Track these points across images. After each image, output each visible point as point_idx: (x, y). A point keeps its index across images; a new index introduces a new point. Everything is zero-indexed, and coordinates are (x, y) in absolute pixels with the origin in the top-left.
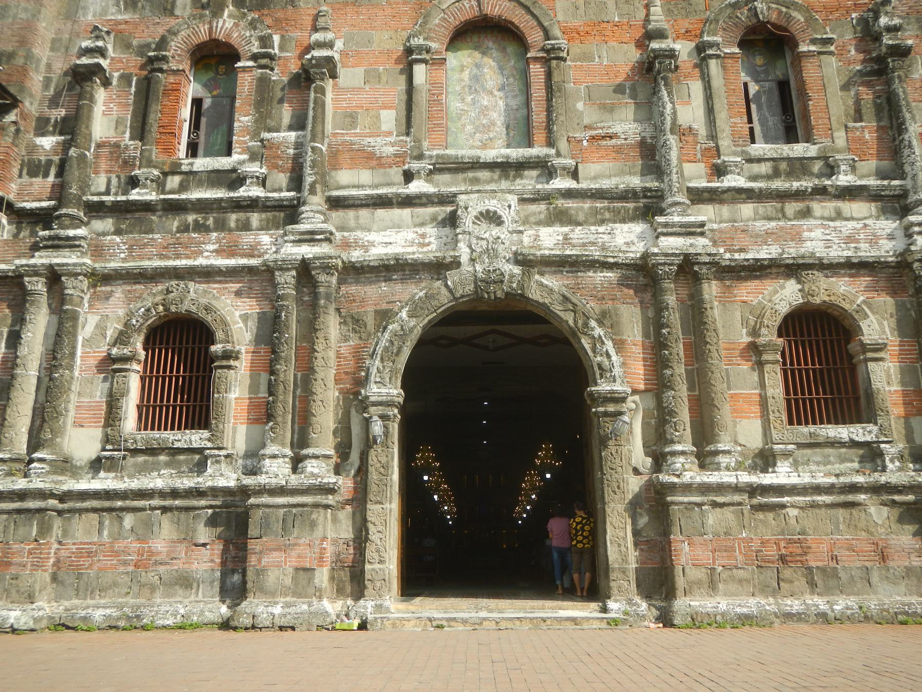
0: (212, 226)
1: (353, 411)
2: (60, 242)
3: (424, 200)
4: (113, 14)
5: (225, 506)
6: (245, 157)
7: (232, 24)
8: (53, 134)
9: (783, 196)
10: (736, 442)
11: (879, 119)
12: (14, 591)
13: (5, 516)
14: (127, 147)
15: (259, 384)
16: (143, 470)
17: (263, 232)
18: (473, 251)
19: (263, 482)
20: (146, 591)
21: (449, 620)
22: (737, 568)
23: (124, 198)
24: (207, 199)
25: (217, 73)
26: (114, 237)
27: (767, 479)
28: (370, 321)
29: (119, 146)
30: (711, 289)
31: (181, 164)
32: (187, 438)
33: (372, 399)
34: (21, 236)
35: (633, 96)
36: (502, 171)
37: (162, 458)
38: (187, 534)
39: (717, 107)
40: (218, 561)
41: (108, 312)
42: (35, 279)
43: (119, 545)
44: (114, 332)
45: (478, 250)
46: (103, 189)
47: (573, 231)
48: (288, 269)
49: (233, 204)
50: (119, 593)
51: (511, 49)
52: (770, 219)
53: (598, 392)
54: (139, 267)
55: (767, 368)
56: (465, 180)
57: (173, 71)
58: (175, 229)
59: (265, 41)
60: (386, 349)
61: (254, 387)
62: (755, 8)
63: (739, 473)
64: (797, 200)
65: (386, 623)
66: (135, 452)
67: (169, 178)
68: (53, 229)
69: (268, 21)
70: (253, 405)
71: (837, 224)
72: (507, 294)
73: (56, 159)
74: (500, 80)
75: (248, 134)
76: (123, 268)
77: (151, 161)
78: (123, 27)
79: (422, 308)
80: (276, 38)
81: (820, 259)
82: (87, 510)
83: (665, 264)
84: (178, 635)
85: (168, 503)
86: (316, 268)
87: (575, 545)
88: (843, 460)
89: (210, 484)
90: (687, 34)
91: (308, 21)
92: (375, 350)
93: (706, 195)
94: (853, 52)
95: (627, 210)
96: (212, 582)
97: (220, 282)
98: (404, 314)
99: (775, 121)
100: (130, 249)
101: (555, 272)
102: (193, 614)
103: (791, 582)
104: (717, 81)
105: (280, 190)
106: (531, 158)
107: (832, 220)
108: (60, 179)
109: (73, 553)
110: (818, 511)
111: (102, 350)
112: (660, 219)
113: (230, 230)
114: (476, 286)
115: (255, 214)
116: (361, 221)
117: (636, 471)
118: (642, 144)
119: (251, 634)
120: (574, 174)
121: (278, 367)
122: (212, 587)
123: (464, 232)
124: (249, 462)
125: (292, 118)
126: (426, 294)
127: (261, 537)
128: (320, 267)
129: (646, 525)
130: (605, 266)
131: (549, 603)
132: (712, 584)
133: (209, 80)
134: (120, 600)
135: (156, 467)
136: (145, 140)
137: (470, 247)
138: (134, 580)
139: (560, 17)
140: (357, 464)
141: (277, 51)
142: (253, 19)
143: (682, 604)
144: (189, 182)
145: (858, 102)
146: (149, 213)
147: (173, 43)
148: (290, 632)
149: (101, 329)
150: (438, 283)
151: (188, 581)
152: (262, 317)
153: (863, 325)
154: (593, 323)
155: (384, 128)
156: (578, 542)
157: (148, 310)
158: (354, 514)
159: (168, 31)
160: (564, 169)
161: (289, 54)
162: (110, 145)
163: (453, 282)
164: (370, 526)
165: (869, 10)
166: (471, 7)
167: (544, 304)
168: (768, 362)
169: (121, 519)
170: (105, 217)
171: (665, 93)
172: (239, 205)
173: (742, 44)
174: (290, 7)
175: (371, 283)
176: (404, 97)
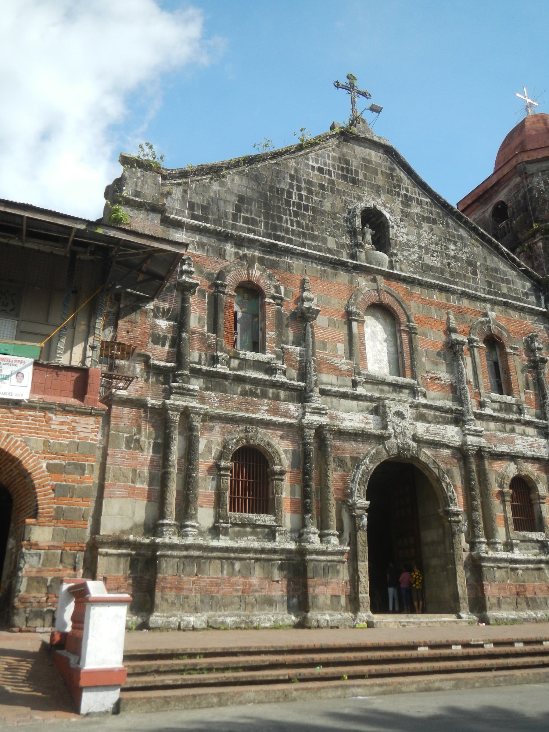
0: (259, 394)
1: (344, 511)
2: (184, 392)
5: (288, 559)
8: (168, 320)
9: (506, 421)
11: (535, 390)
12: (186, 606)
13: (177, 560)
14: (209, 337)
15: (295, 491)
16: (239, 535)
18: (395, 432)
19: (316, 547)
20: (249, 607)
21: (408, 622)
22: (507, 597)
23: (214, 369)
24: (259, 379)
25: (243, 298)
26: (211, 392)
27: (510, 555)
28: (348, 461)
29: (204, 335)
31: (239, 354)
32: (263, 518)
33: (358, 505)
34: (150, 380)
35: (445, 360)
36: (394, 388)
37: (248, 529)
38: (268, 575)
39: (478, 372)
40: (285, 590)
41: (212, 438)
42: (175, 413)
43: (234, 579)
44: (216, 451)
45: (398, 432)
46: (197, 360)
48: (312, 429)
49: (272, 384)
50: (235, 608)
52: (500, 431)
53: (452, 510)
54: (233, 415)
56: (377, 389)
57: (231, 295)
58: (239, 393)
60: (361, 478)
61: (292, 493)
62: (490, 326)
64: (510, 424)
65: (382, 624)
66: (235, 525)
67: (232, 360)
69: (277, 277)
70: (293, 503)
72: (412, 456)
73: (169, 336)
74: (385, 336)
75: (274, 343)
76: (224, 414)
77: (223, 348)
78: (197, 259)
79: (375, 459)
80: (282, 288)
81: (524, 454)
82: (215, 558)
83: (471, 450)
84: (273, 631)
85: (258, 556)
86: (326, 430)
87: (415, 587)
88: (534, 548)
89: (282, 546)
91: (298, 283)
92: (354, 479)
94: (524, 356)
95: (448, 418)
96: (283, 603)
97: (272, 429)
98: (367, 460)
100: (220, 401)
101: (428, 447)
102: (279, 620)
103: (521, 604)
105: (293, 379)
106: (407, 384)
107: (522, 435)
108: (172, 349)
109: (208, 584)
110: (528, 571)
111: (211, 461)
113: (269, 399)
114: (399, 451)
115: (282, 391)
116: (334, 404)
117: (464, 551)
118: (451, 385)
119: (318, 630)
120: (425, 396)
121: (311, 483)
122: (283, 606)
123: (391, 421)
124: (293, 535)
125: (294, 337)
126: (376, 451)
127: (313, 578)
128: (328, 430)
130: (448, 447)
131: (437, 615)
132: (499, 605)
133: (239, 301)
134: (236, 612)
135: (245, 534)
136: (218, 335)
137: (394, 429)
138: (242, 601)
139: (412, 311)
140: (348, 539)
142: (270, 274)
143: (491, 614)
144: (243, 364)
145: (527, 380)
146: (224, 380)
148: (336, 630)
150: (381, 446)
151: (270, 601)
152: (294, 452)
153: (539, 486)
154: (446, 476)
156: (416, 585)
157: (238, 441)
158: (349, 566)
159: (225, 268)
160: (422, 392)
162: (199, 333)
163: (388, 447)
164: (360, 573)
165: (529, 337)
166: (375, 295)
167: (426, 464)
169: (233, 565)
170: (199, 378)
171: (462, 362)
173: (484, 342)
175: (347, 441)
176: (347, 338)
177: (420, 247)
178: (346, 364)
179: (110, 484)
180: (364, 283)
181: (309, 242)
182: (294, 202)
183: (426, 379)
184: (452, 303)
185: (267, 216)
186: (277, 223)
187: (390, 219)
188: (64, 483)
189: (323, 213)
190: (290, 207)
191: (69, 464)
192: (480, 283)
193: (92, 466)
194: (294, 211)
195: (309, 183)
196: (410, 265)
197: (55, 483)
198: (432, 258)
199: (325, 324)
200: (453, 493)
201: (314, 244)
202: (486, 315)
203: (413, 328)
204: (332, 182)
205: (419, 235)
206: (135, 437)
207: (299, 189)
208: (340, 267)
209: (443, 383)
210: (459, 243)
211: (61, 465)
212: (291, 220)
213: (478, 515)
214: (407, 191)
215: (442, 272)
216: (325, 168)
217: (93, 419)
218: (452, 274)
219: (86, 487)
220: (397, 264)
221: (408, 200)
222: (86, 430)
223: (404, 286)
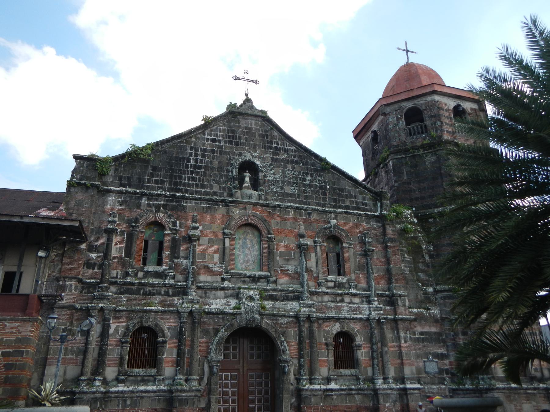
3: (228, 289)
4: (117, 206)
6: (167, 268)
10: (320, 375)
25: (154, 231)
28: (211, 332)
30: (315, 327)
34: (84, 292)
39: (319, 263)
46: (115, 275)
47: (275, 303)
51: (256, 233)
52: (332, 302)
55: (330, 351)
56: (241, 281)
59: (175, 224)
68: (100, 292)
71: (351, 305)
78: (121, 211)
80: (178, 223)
90: (311, 237)
99: (334, 266)
104: (319, 254)
105: (180, 282)
112: (301, 302)
113: (162, 295)
117: (292, 384)
120: (275, 282)
129: (294, 402)
139: (273, 226)
141: (178, 228)
149: (116, 330)
155: (215, 260)
157: (135, 325)
163: (239, 320)
166: (245, 219)
167: (267, 329)
168: (330, 349)
169: (125, 401)
172: (165, 286)
174: (183, 212)
177: (283, 182)
179: (51, 358)
180: (238, 212)
181: (200, 189)
182: (191, 165)
185: (171, 177)
186: (178, 180)
187: (260, 166)
188: (11, 362)
189: (212, 169)
190: (188, 168)
191: (14, 351)
192: (328, 201)
193: (28, 351)
194: (191, 171)
195: (205, 150)
196: (274, 195)
197: (5, 362)
198: (291, 188)
199: (206, 242)
200: (285, 346)
201: (203, 190)
202: (329, 223)
203: (271, 238)
204: (221, 147)
205: (284, 173)
206: (68, 328)
207: (196, 155)
208: (221, 203)
211: (10, 352)
212: (188, 177)
213: (305, 361)
214: (278, 144)
215: (299, 196)
217: (31, 323)
218: (306, 197)
219: (24, 363)
220: (263, 196)
221: (277, 151)
222: (26, 330)
223: (268, 209)
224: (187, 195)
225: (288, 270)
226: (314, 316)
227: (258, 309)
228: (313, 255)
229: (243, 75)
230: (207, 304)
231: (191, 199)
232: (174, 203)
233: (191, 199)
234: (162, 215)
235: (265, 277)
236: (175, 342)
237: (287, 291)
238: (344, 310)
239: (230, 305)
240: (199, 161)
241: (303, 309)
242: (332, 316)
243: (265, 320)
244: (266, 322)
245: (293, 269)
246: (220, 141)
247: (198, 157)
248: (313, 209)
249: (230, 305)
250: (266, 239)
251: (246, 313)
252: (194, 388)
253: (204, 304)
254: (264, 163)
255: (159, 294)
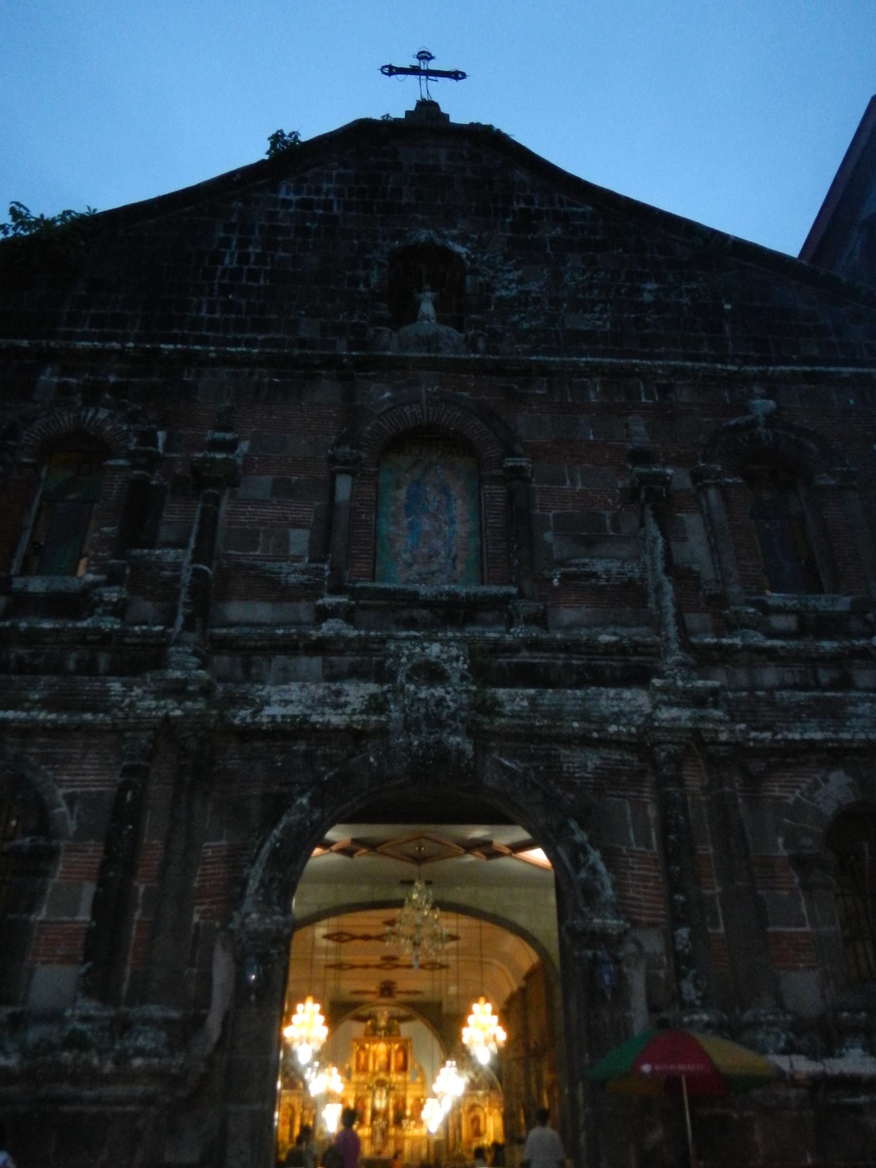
3: (342, 645)
7: (105, 415)
17: (115, 678)
47: (541, 694)
63: (794, 1057)
80: (161, 435)
83: (669, 742)
93: (716, 655)
112: (657, 682)
120: (540, 620)
141: (160, 450)
147: (25, 432)
161: (175, 455)
163: (377, 758)
172: (81, 638)
178: (303, 572)
180: (387, 395)
183: (550, 580)
184: (643, 400)
198: (587, 316)
200: (593, 870)
202: (747, 411)
203: (517, 471)
207: (244, 244)
208: (324, 372)
209: (603, 583)
210: (670, 277)
214: (529, 201)
216: (316, 198)
224: (198, 347)
225: (595, 575)
226: (723, 737)
227: (463, 714)
228: (693, 522)
229: (415, 62)
230: (245, 701)
231: (214, 363)
232: (155, 379)
233: (214, 363)
234: (103, 414)
235: (499, 603)
236: (94, 849)
237: (591, 648)
238: (858, 716)
239: (345, 704)
240: (252, 259)
241: (665, 714)
242: (807, 736)
243: (495, 755)
244: (502, 765)
245: (614, 570)
246: (327, 205)
247: (251, 249)
248: (674, 372)
249: (345, 704)
250: (500, 472)
251: (410, 726)
252: (138, 1062)
253: (234, 701)
254: (483, 254)
255: (57, 668)
